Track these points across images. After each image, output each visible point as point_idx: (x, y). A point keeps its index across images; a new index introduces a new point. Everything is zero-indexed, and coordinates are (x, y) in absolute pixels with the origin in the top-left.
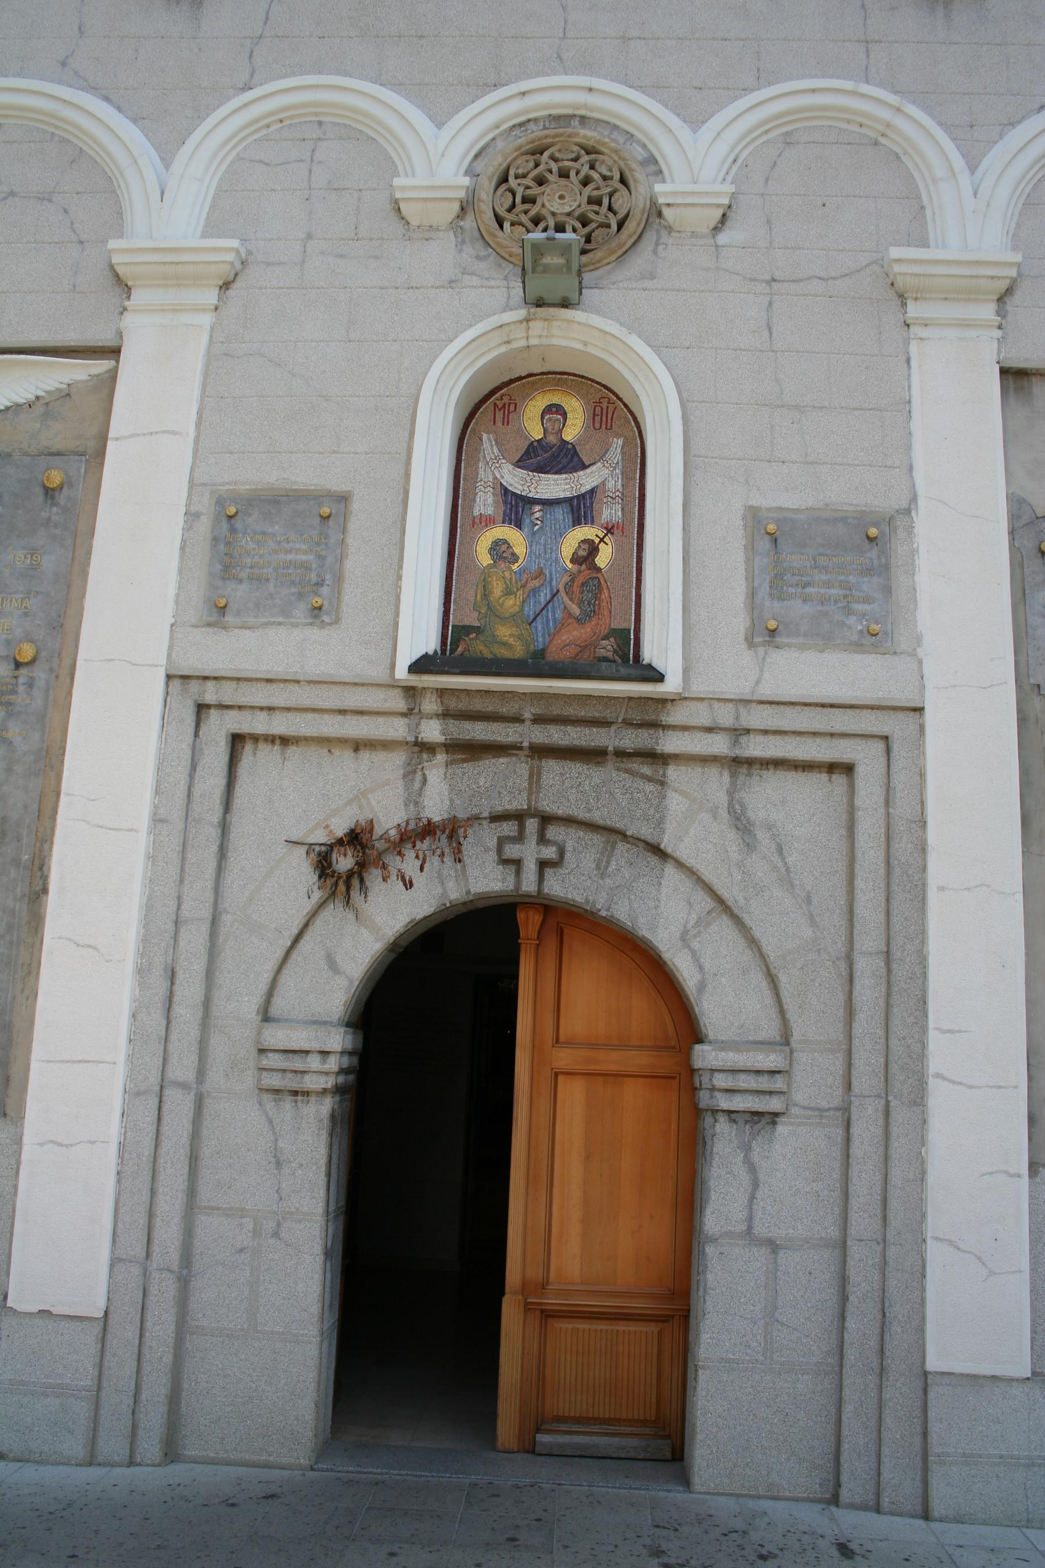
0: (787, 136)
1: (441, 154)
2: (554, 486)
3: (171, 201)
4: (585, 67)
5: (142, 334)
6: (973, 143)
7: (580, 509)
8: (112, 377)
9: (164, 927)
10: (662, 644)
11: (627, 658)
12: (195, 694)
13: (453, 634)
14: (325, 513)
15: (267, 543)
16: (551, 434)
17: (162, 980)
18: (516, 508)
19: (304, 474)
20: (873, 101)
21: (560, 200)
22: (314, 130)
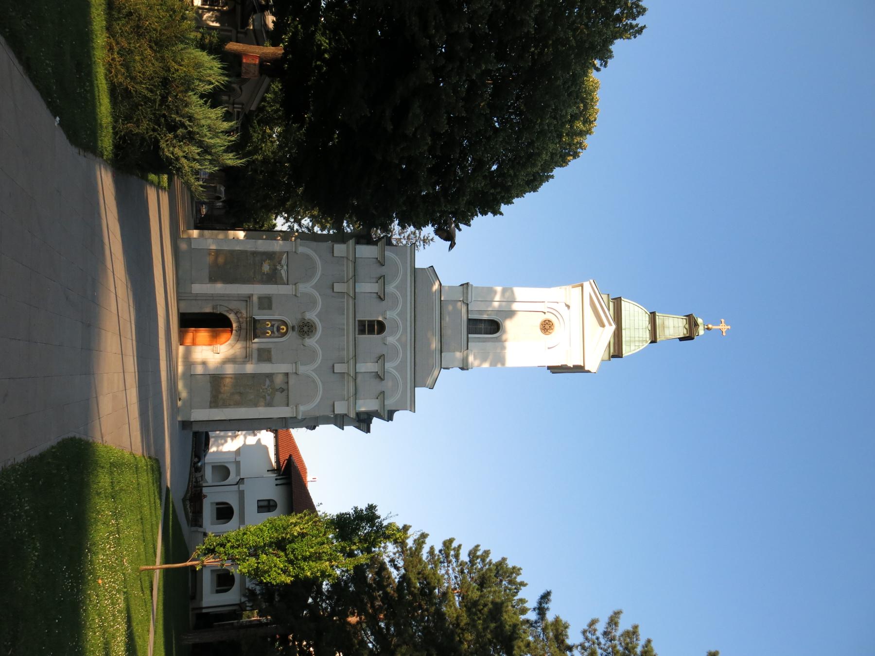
0: (314, 352)
1: (312, 316)
2: (275, 329)
3: (305, 288)
4: (323, 330)
5: (289, 287)
6: (315, 370)
7: (273, 332)
8: (284, 284)
9: (228, 296)
10: (256, 340)
11: (255, 337)
12: (250, 297)
13: (259, 320)
14: (270, 307)
15: (266, 302)
16: (279, 328)
17: (223, 296)
18: (272, 326)
19: (274, 306)
20: (319, 361)
21: (305, 329)
22: (314, 303)
